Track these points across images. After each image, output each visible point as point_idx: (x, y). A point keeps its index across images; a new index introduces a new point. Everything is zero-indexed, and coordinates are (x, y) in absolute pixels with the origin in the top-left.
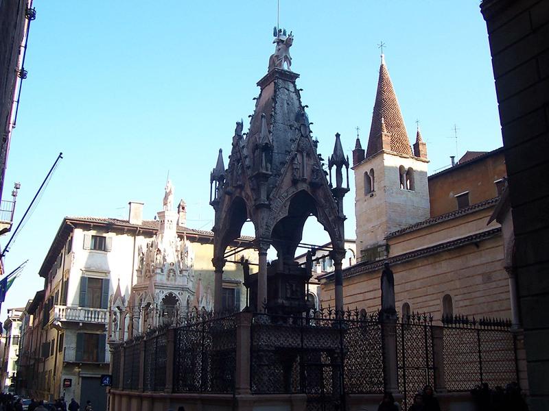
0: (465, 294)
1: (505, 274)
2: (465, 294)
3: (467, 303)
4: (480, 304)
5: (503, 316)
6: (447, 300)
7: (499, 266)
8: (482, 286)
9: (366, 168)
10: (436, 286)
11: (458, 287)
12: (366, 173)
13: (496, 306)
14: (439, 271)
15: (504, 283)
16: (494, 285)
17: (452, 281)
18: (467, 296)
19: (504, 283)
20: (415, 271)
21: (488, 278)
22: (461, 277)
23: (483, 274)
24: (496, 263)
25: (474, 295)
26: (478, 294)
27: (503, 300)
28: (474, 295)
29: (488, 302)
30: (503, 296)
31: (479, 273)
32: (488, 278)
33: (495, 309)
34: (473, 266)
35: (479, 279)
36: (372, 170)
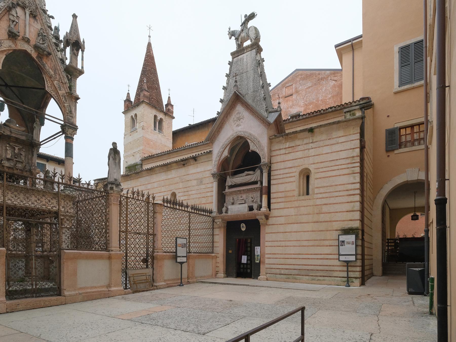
1: (212, 179)
3: (186, 198)
5: (208, 207)
7: (208, 174)
8: (197, 187)
9: (132, 113)
12: (132, 116)
13: (204, 201)
15: (210, 185)
18: (186, 193)
19: (210, 185)
20: (154, 176)
21: (200, 181)
24: (207, 172)
25: (190, 193)
26: (193, 192)
28: (190, 193)
29: (199, 198)
30: (209, 194)
32: (200, 181)
33: (203, 203)
35: (194, 183)
36: (136, 115)
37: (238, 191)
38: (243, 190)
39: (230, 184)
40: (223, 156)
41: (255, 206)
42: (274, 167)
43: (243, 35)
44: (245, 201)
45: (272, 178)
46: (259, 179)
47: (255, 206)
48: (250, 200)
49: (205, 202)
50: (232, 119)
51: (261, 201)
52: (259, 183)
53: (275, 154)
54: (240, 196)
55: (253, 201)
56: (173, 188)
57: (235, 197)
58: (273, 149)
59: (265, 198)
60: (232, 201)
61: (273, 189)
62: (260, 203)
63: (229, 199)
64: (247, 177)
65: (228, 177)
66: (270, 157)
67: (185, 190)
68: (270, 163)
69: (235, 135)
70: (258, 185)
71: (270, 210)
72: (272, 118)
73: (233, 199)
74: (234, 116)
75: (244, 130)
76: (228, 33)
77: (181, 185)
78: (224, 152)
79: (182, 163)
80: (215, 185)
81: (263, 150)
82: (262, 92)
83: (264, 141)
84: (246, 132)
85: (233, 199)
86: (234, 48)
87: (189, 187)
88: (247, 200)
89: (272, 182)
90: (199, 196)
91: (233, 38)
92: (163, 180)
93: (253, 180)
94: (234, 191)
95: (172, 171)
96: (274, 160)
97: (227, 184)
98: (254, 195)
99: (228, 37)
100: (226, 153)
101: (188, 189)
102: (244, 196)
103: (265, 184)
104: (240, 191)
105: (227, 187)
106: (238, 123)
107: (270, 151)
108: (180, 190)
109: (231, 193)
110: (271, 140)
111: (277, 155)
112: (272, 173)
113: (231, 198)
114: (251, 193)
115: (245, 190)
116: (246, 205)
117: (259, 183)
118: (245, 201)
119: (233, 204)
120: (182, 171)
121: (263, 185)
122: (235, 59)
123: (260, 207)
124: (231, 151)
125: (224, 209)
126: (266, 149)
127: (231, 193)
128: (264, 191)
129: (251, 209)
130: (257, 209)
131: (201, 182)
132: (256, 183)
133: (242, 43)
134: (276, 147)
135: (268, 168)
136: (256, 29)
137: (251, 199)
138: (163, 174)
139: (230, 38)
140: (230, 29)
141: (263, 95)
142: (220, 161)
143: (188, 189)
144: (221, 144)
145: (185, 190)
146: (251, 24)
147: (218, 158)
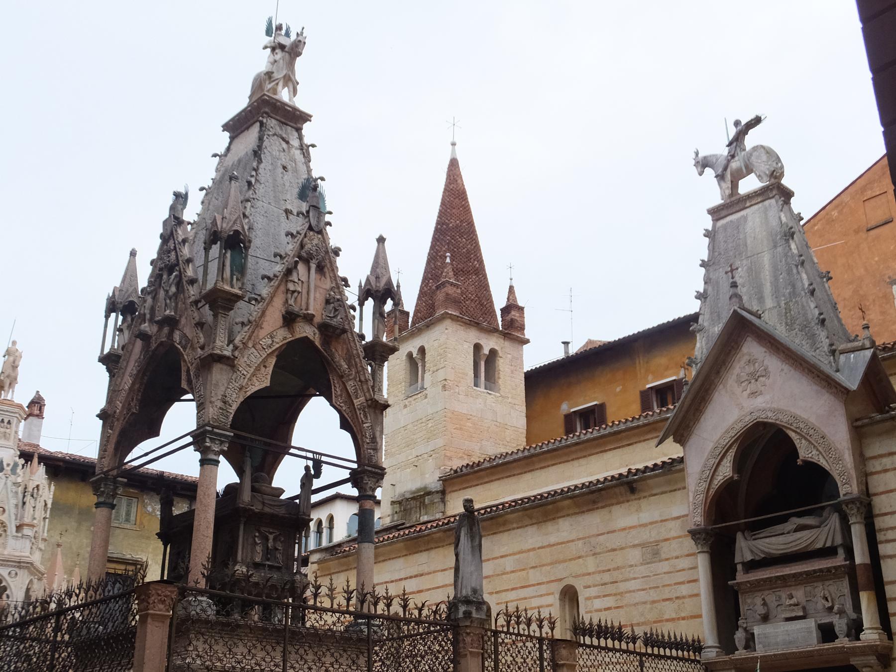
0: (605, 584)
1: (689, 544)
2: (605, 584)
3: (610, 602)
4: (636, 604)
6: (570, 596)
7: (674, 529)
8: (642, 568)
10: (548, 568)
11: (591, 570)
13: (669, 610)
14: (553, 539)
16: (665, 567)
17: (579, 557)
18: (611, 589)
19: (685, 563)
21: (653, 552)
22: (598, 550)
23: (642, 545)
25: (623, 587)
27: (684, 597)
28: (623, 587)
29: (653, 602)
30: (684, 590)
31: (636, 542)
32: (653, 552)
33: (666, 617)
34: (624, 529)
35: (635, 555)
37: (778, 578)
38: (794, 575)
39: (749, 557)
40: (719, 479)
41: (840, 625)
42: (881, 504)
43: (734, 165)
44: (804, 608)
45: (880, 537)
46: (839, 540)
47: (840, 625)
48: (820, 606)
49: (674, 616)
50: (734, 377)
51: (857, 607)
52: (841, 551)
53: (879, 468)
54: (784, 594)
55: (830, 609)
56: (567, 573)
57: (771, 599)
58: (869, 453)
59: (866, 600)
60: (761, 610)
61: (891, 570)
62: (854, 616)
63: (751, 605)
64: (799, 535)
65: (739, 535)
66: (865, 476)
67: (607, 577)
68: (868, 495)
69: (748, 420)
70: (840, 560)
71: (890, 637)
72: (852, 371)
73: (765, 604)
74: (738, 368)
75: (775, 406)
76: (693, 162)
77: (591, 564)
78: (720, 468)
79: (591, 497)
80: (702, 564)
81: (839, 459)
82: (812, 305)
83: (839, 434)
84: (780, 411)
85: (765, 604)
86: (716, 199)
87: (618, 568)
88: (811, 608)
89: (883, 549)
90: (654, 595)
91: (709, 172)
92: (534, 549)
93: (819, 545)
94: (765, 580)
95: (561, 521)
96: (878, 483)
97: (738, 559)
98: (832, 589)
99: (695, 171)
100: (726, 470)
101: (616, 575)
102: (799, 594)
103: (860, 556)
104: (783, 578)
105: (739, 567)
106: (753, 387)
107: (861, 459)
108: (588, 580)
109: (757, 586)
110: (860, 432)
111: (886, 471)
112: (879, 523)
113: (759, 601)
114: (820, 584)
115: (801, 574)
116: (810, 624)
117: (841, 551)
118: (804, 608)
119: (765, 619)
120: (592, 522)
121: (858, 560)
122: (720, 223)
123: (856, 628)
124: (739, 465)
125: (740, 635)
126: (848, 459)
127: (757, 586)
128: (861, 579)
129: (827, 633)
130: (848, 635)
131: (656, 553)
132: (828, 552)
133: (734, 186)
134: (875, 448)
135: (863, 510)
136: (769, 152)
137: (821, 604)
138: (531, 530)
139: (701, 174)
140: (697, 154)
141: (817, 312)
142: (712, 492)
143: (616, 575)
144: (710, 446)
145: (607, 577)
146: (751, 140)
147: (705, 485)
